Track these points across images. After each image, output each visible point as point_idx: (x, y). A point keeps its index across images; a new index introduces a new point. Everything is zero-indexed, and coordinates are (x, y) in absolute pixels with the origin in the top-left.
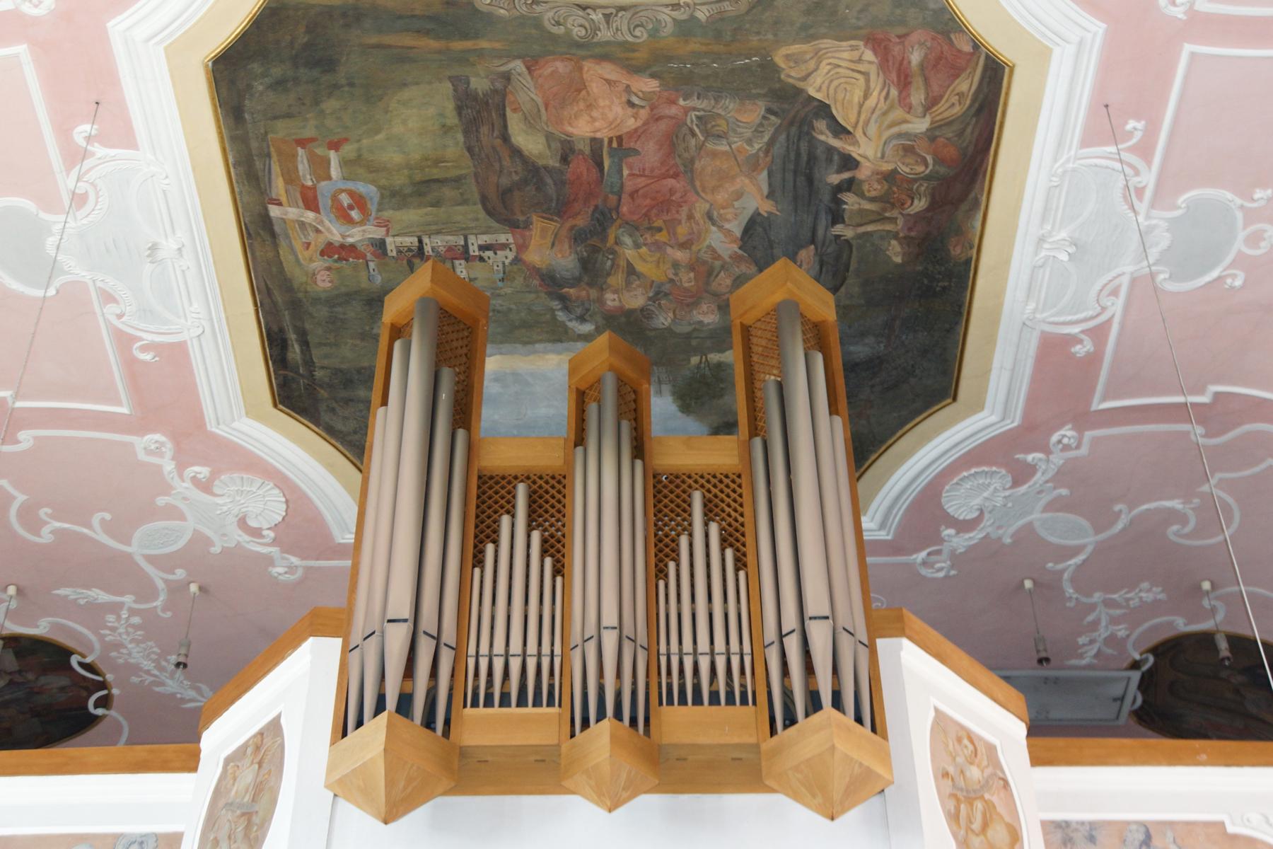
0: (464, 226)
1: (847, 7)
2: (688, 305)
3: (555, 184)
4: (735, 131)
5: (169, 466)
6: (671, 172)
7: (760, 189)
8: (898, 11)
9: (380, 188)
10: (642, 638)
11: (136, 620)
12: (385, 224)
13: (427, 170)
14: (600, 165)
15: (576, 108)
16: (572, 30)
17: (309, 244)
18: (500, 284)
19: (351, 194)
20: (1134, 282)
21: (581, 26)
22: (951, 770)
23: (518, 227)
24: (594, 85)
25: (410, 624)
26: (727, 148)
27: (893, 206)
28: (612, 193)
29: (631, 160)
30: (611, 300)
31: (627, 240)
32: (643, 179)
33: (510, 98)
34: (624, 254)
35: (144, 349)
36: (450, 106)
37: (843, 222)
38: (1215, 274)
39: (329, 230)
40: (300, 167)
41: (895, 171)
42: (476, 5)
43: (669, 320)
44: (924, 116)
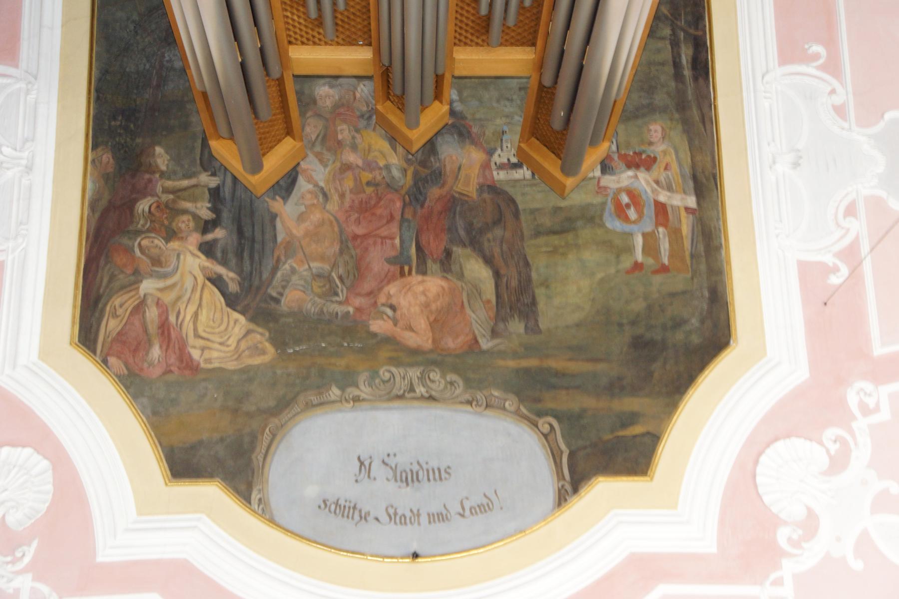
0: (534, 188)
1: (216, 399)
2: (343, 105)
3: (457, 230)
4: (306, 281)
6: (359, 241)
7: (283, 223)
8: (173, 395)
9: (602, 225)
12: (601, 190)
13: (563, 244)
14: (419, 248)
15: (438, 303)
16: (441, 377)
17: (666, 169)
18: (506, 128)
19: (626, 219)
21: (433, 381)
23: (489, 186)
24: (423, 326)
26: (312, 265)
27: (167, 206)
28: (408, 221)
29: (393, 253)
31: (396, 173)
32: (383, 235)
33: (492, 314)
34: (399, 160)
36: (541, 305)
37: (209, 190)
39: (648, 183)
40: (667, 245)
41: (168, 240)
42: (517, 399)
43: (359, 89)
44: (145, 295)
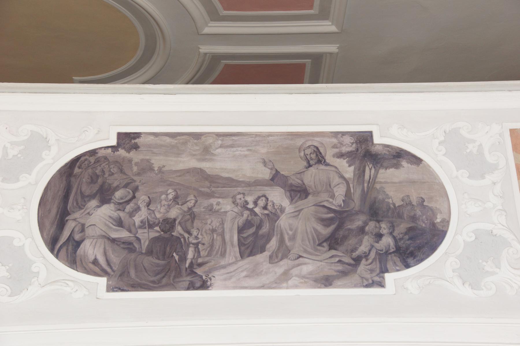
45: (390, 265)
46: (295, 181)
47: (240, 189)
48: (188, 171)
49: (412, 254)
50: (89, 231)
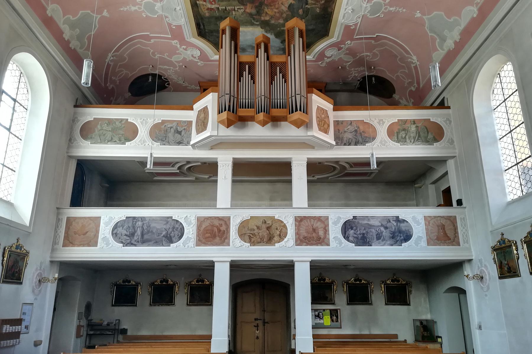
5: (179, 46)
10: (268, 97)
11: (173, 71)
12: (219, 5)
17: (204, 8)
20: (363, 16)
22: (319, 116)
25: (229, 94)
30: (263, 18)
31: (266, 8)
35: (174, 26)
37: (308, 5)
38: (378, 15)
45: (403, 242)
46: (385, 226)
47: (375, 227)
48: (366, 224)
49: (407, 240)
50: (350, 235)
